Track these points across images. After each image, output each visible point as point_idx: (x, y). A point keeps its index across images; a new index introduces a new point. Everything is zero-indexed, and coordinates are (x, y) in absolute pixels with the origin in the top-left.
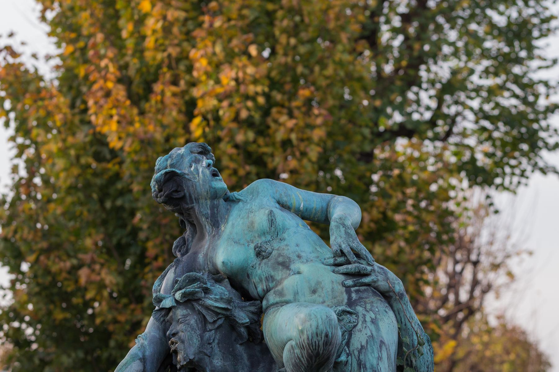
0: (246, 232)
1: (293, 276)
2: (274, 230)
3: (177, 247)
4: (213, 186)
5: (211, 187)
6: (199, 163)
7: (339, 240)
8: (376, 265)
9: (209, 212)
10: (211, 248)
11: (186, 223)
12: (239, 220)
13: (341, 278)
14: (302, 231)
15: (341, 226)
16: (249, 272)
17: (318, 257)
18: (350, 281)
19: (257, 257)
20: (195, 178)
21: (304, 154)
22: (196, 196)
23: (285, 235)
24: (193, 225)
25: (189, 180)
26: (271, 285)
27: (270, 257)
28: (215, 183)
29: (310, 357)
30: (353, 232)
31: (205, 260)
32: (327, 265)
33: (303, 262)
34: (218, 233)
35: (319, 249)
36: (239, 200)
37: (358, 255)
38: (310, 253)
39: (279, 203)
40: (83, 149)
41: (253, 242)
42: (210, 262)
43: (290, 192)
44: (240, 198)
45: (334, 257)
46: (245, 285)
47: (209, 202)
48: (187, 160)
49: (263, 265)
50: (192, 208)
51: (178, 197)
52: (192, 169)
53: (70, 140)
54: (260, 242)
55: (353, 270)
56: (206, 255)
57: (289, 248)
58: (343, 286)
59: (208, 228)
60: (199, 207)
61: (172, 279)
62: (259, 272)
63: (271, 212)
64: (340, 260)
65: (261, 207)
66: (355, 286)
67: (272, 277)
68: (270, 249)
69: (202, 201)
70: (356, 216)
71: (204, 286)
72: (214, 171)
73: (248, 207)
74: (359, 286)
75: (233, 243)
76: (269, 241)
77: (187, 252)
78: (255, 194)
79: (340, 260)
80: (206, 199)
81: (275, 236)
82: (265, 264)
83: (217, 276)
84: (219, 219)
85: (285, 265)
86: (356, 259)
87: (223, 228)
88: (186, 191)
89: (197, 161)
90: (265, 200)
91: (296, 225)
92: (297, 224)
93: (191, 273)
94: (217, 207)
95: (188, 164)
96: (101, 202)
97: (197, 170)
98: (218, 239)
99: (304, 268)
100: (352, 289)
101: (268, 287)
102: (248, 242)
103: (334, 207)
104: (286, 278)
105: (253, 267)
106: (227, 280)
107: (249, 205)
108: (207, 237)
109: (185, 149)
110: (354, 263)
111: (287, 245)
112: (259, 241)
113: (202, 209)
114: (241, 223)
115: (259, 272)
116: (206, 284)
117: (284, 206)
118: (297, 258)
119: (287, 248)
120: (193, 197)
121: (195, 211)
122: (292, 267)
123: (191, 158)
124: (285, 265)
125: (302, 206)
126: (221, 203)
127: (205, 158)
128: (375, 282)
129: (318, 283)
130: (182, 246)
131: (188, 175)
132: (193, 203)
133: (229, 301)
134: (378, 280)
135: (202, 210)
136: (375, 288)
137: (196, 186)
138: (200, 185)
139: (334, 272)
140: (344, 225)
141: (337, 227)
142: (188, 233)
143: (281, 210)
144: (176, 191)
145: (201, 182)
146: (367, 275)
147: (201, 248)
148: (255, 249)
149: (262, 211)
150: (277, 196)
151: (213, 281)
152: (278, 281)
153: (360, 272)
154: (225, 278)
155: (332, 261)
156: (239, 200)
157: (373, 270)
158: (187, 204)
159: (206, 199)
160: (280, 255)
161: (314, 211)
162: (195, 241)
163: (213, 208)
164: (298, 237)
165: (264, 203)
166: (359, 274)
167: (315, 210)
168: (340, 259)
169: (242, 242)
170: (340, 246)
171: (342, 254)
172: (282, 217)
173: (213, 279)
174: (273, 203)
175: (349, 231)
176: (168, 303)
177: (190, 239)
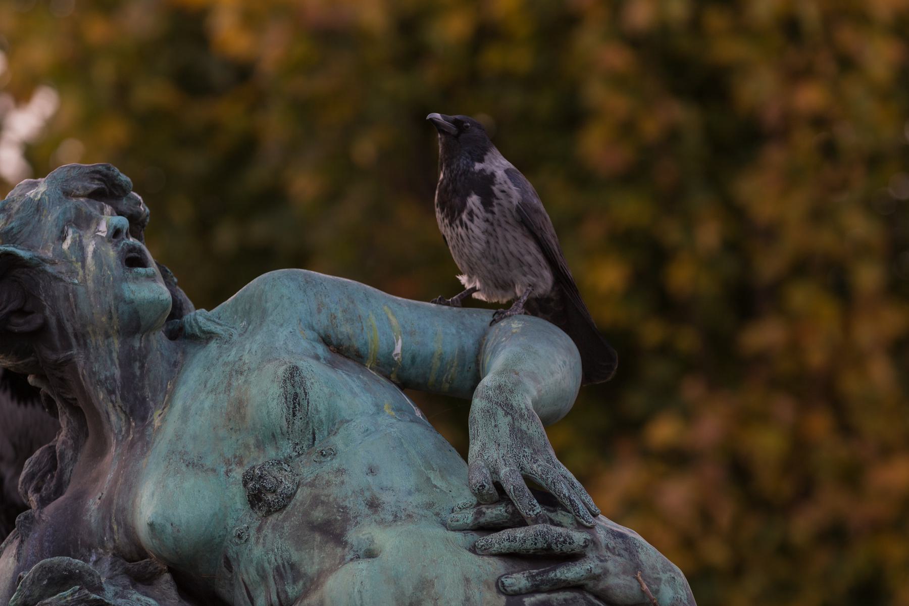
0: (222, 432)
1: (350, 566)
2: (304, 426)
3: (31, 477)
4: (127, 294)
5: (119, 298)
6: (88, 227)
7: (493, 454)
8: (605, 522)
9: (117, 372)
10: (121, 481)
11: (59, 404)
12: (202, 396)
13: (495, 567)
14: (391, 425)
15: (501, 412)
16: (231, 553)
17: (430, 506)
18: (519, 576)
19: (253, 506)
20: (73, 273)
21: (847, 64)
22: (78, 326)
23: (337, 441)
24: (75, 410)
25: (56, 278)
26: (292, 590)
27: (289, 508)
28: (133, 287)
30: (536, 429)
31: (104, 518)
32: (454, 530)
33: (382, 523)
34: (142, 434)
35: (437, 482)
36: (210, 336)
37: (547, 498)
38: (410, 493)
39: (326, 340)
40: (144, 55)
41: (240, 463)
42: (119, 524)
43: (361, 309)
44: (212, 327)
45: (479, 504)
46: (223, 590)
47: (116, 344)
48: (51, 218)
49: (267, 531)
50: (69, 361)
51: (25, 328)
52: (66, 246)
53: (97, 30)
54: (260, 462)
55: (528, 545)
56: (107, 503)
57: (346, 478)
58: (499, 591)
59: (115, 419)
60: (87, 358)
61: (10, 575)
62: (258, 552)
63: (293, 372)
64: (494, 513)
65: (268, 355)
66: (535, 590)
67: (292, 566)
68: (287, 484)
69: (96, 340)
70: (558, 376)
71: (94, 596)
72: (133, 249)
73: (231, 358)
74: (550, 591)
75: (184, 468)
76: (288, 460)
77: (59, 491)
78: (255, 315)
79: (494, 513)
80: (107, 336)
81: (305, 444)
82: (274, 528)
84: (148, 393)
85: (331, 531)
86: (539, 509)
87: (157, 422)
88: (48, 312)
89: (82, 221)
90: (282, 334)
91: (374, 409)
92: (377, 405)
93: (56, 559)
94: (143, 356)
95: (55, 231)
96: (203, 227)
97: (79, 247)
98: (143, 454)
99: (387, 539)
100: (528, 600)
101: (283, 597)
102: (228, 463)
103: (494, 352)
104: (332, 570)
105: (239, 537)
106: (167, 576)
107: (233, 353)
108: (113, 451)
109: (50, 183)
110: (536, 521)
111: (340, 471)
112: (257, 459)
113: (100, 364)
114: (207, 404)
115: (258, 552)
116: (99, 589)
117: (341, 351)
118: (365, 510)
119: (338, 480)
120: (70, 330)
121: (74, 369)
122: (354, 536)
123: (64, 213)
125: (398, 349)
126: (155, 344)
127: (108, 209)
128: (596, 578)
129: (425, 584)
130: (45, 475)
131: (53, 263)
132: (69, 347)
134: (606, 572)
135: (96, 367)
136: (597, 597)
137: (75, 296)
138: (87, 292)
139: (473, 549)
140: (509, 409)
141: (489, 414)
142: (62, 439)
143: (332, 365)
144: (21, 312)
145: (90, 284)
146: (573, 557)
147: (96, 480)
148: (245, 484)
149: (270, 368)
150: (322, 321)
151: (126, 581)
152: (312, 580)
153: (549, 548)
154: (161, 572)
155: (468, 517)
156: (210, 336)
157: (594, 543)
158: (54, 349)
159: (107, 336)
160: (316, 501)
161: (436, 364)
162: (82, 457)
163: (128, 360)
164: (374, 442)
165: (280, 343)
167: (441, 358)
168: (494, 511)
169: (208, 462)
170: (495, 472)
171: (501, 494)
173: (127, 572)
174: (304, 344)
175: (524, 427)
177: (69, 453)
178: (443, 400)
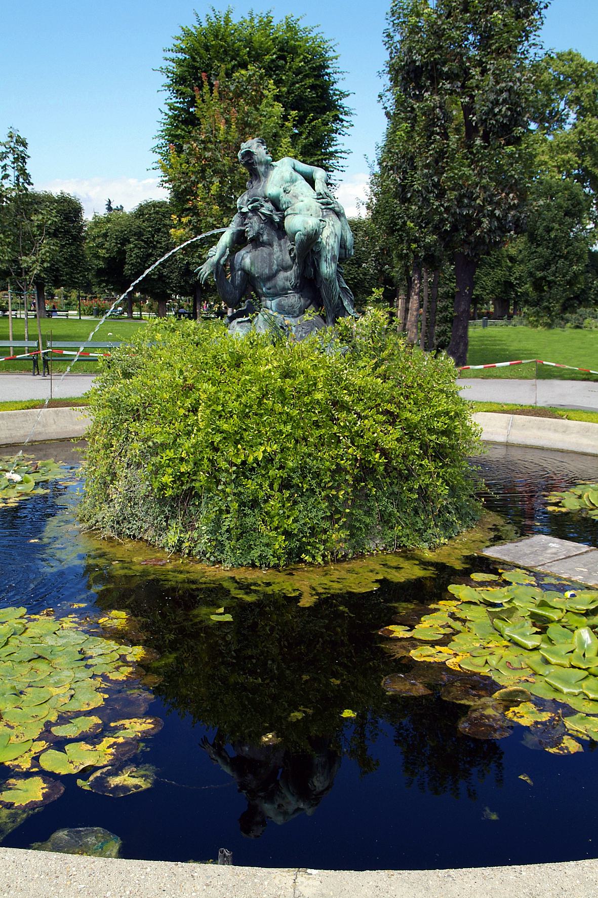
29: (308, 239)
133: (271, 211)
166: (328, 204)
172: (295, 174)
176: (245, 210)
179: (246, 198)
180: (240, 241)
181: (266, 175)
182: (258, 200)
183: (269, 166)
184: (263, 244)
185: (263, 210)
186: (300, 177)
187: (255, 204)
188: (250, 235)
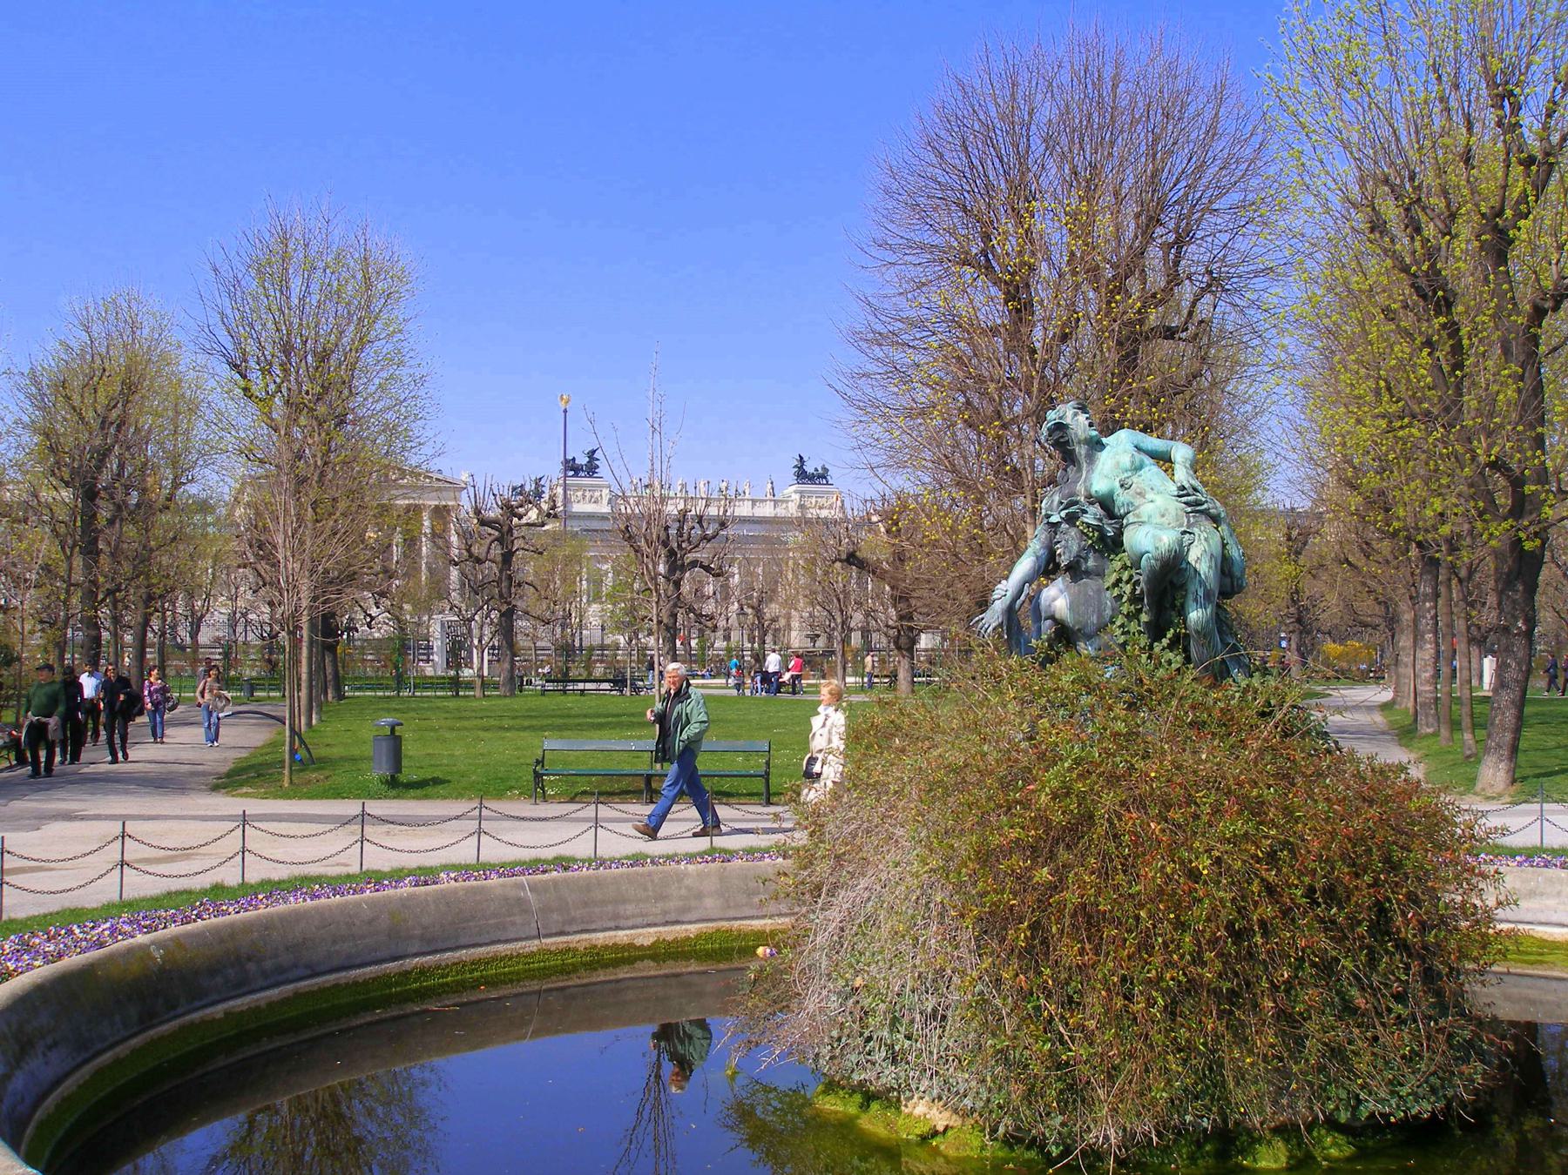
37: (1195, 490)
83: (1091, 499)
85: (1141, 494)
113: (1081, 451)
124: (1141, 494)
171: (1183, 488)
178: (1164, 460)
179: (1057, 498)
180: (1049, 568)
181: (1091, 459)
182: (1076, 503)
183: (1096, 445)
184: (1088, 573)
185: (1088, 519)
186: (1147, 460)
187: (1071, 510)
188: (1064, 561)
